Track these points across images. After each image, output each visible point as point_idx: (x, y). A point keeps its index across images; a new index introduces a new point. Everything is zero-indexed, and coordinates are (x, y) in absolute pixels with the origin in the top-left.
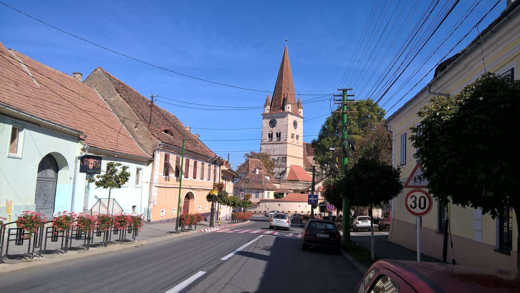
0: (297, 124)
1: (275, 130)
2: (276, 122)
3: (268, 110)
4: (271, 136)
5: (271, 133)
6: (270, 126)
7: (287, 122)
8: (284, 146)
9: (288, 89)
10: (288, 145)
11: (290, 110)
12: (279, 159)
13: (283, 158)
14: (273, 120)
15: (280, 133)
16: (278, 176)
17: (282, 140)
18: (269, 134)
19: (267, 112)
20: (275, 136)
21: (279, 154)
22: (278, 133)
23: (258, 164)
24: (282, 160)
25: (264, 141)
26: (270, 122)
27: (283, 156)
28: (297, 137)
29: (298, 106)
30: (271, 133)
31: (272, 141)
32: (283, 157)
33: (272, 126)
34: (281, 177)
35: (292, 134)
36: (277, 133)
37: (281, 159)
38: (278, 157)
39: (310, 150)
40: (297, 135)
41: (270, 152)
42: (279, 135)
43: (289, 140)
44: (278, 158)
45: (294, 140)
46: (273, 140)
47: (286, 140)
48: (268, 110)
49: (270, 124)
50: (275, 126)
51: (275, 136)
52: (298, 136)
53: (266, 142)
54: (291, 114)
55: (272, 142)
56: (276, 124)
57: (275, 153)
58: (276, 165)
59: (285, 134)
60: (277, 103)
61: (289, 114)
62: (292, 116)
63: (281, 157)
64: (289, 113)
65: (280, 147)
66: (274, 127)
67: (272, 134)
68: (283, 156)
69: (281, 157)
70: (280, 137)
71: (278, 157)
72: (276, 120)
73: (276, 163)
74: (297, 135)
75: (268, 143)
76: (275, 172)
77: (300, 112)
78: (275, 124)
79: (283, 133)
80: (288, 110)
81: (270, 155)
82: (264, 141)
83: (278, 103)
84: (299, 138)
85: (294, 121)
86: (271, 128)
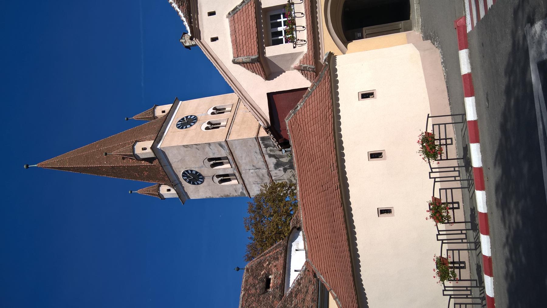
0: (187, 117)
1: (206, 171)
2: (187, 171)
3: (169, 190)
4: (225, 178)
6: (202, 182)
7: (178, 147)
8: (236, 147)
9: (106, 154)
10: (231, 138)
11: (149, 144)
12: (272, 153)
13: (266, 146)
15: (210, 160)
17: (223, 153)
18: (221, 181)
19: (173, 191)
21: (260, 156)
22: (212, 162)
23: (254, 286)
24: (272, 148)
25: (241, 190)
26: (194, 184)
27: (262, 146)
28: (219, 111)
29: (151, 119)
30: (217, 180)
31: (234, 175)
35: (207, 128)
37: (271, 150)
38: (267, 157)
40: (213, 113)
41: (263, 175)
42: (216, 162)
43: (218, 135)
44: (270, 156)
46: (230, 172)
47: (220, 145)
48: (169, 190)
49: (198, 184)
50: (197, 173)
52: (215, 109)
53: (240, 186)
54: (158, 140)
55: (237, 174)
56: (192, 171)
57: (261, 164)
58: (289, 158)
59: (207, 149)
60: (146, 174)
61: (158, 147)
62: (165, 134)
63: (264, 150)
64: (153, 148)
65: (242, 157)
66: (200, 175)
68: (262, 146)
69: (264, 150)
70: (219, 159)
71: (267, 157)
72: (184, 173)
73: (285, 160)
75: (241, 182)
77: (164, 112)
78: (194, 172)
79: (207, 153)
80: (149, 150)
81: (268, 175)
82: (241, 190)
83: (146, 171)
84: (219, 105)
85: (179, 127)
86: (205, 181)
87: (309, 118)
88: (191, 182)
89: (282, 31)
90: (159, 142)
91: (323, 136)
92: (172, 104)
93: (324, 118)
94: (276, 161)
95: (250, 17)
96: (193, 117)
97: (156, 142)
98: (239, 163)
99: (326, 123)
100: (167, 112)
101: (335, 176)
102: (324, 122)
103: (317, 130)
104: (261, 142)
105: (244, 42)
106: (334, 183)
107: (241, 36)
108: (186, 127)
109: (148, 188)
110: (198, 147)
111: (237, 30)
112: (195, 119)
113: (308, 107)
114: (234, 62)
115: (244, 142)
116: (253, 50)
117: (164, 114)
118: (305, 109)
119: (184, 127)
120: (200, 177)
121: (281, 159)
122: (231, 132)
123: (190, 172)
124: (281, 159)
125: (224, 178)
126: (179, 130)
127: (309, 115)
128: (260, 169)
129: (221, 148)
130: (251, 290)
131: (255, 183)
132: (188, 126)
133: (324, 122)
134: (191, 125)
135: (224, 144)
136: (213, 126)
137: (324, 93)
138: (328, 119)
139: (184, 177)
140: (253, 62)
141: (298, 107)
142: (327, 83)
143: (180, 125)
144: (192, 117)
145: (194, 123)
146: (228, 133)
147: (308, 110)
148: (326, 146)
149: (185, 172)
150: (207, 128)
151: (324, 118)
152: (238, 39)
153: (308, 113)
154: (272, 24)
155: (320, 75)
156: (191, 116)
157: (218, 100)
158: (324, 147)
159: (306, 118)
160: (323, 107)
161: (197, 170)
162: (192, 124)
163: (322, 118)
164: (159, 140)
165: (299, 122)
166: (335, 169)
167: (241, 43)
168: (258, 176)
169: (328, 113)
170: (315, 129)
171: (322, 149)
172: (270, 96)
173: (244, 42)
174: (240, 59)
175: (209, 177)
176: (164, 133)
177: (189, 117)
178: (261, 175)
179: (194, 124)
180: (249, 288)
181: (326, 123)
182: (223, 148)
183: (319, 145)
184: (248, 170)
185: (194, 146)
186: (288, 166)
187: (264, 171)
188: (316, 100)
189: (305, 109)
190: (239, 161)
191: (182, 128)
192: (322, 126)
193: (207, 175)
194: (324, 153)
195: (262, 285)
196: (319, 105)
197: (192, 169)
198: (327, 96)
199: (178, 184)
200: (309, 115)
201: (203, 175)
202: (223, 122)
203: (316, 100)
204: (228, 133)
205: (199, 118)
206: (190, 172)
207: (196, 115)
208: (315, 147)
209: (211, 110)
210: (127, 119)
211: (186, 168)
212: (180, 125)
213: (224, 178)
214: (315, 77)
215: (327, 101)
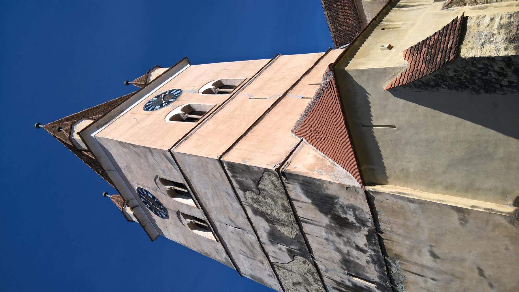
16: (361, 239)
27: (236, 185)
32: (238, 182)
34: (363, 223)
39: (348, 25)
61: (93, 135)
63: (240, 193)
69: (240, 193)
76: (338, 250)
90: (102, 126)
94: (269, 228)
97: (96, 124)
109: (115, 196)
110: (136, 149)
121: (279, 227)
124: (279, 227)
128: (244, 230)
131: (242, 253)
149: (139, 190)
164: (104, 123)
168: (243, 242)
176: (123, 111)
178: (249, 243)
184: (224, 225)
185: (131, 147)
186: (296, 248)
187: (253, 238)
199: (138, 206)
210: (127, 84)
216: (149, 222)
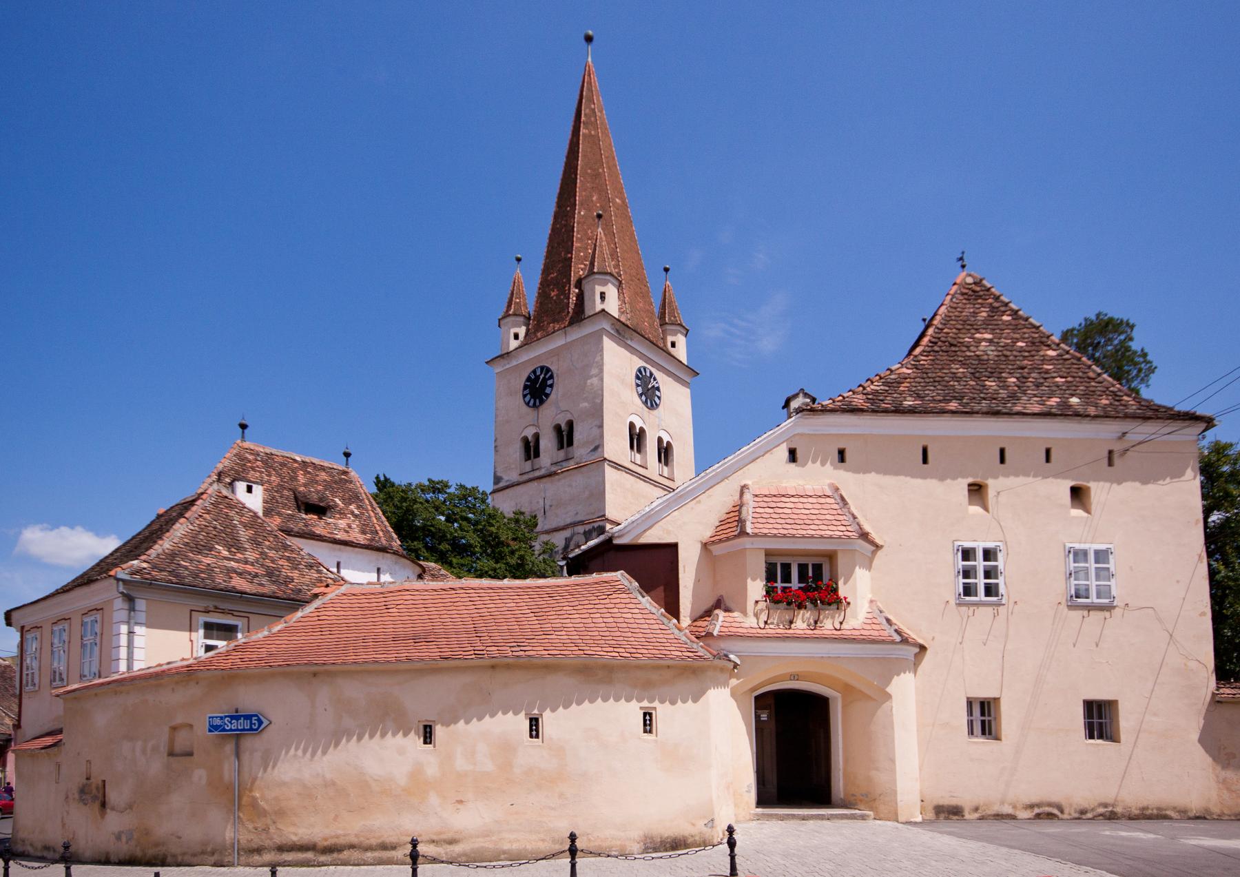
0: (658, 389)
2: (552, 377)
5: (529, 433)
6: (528, 404)
14: (538, 373)
15: (570, 424)
17: (580, 450)
18: (526, 442)
20: (548, 443)
22: (563, 426)
23: (313, 481)
26: (525, 387)
28: (665, 453)
33: (535, 403)
35: (632, 426)
36: (558, 428)
40: (660, 440)
42: (565, 436)
43: (616, 445)
45: (644, 458)
49: (525, 396)
50: (547, 396)
51: (548, 443)
56: (551, 386)
66: (542, 402)
67: (537, 437)
70: (570, 443)
74: (660, 440)
77: (673, 345)
78: (548, 390)
85: (639, 371)
87: (619, 615)
88: (529, 383)
89: (790, 582)
91: (581, 637)
92: (686, 364)
93: (615, 642)
95: (825, 527)
96: (658, 401)
98: (559, 480)
99: (605, 645)
100: (672, 350)
101: (500, 652)
102: (607, 642)
103: (595, 629)
104: (596, 525)
105: (780, 511)
106: (488, 649)
107: (792, 505)
108: (638, 385)
111: (802, 500)
112: (652, 405)
113: (640, 616)
114: (743, 489)
115: (599, 494)
116: (761, 526)
117: (669, 345)
118: (637, 611)
119: (639, 382)
120: (537, 401)
122: (619, 472)
123: (549, 382)
125: (532, 449)
126: (635, 371)
127: (624, 615)
129: (592, 447)
130: (304, 475)
132: (640, 389)
133: (607, 642)
134: (641, 395)
135: (596, 456)
136: (637, 439)
137: (663, 648)
138: (612, 649)
139: (539, 369)
140: (741, 522)
141: (643, 597)
142: (680, 654)
143: (644, 374)
144: (656, 399)
145: (645, 403)
146: (617, 466)
147: (634, 616)
148: (562, 641)
149: (550, 373)
150: (632, 426)
151: (615, 642)
152: (784, 499)
153: (629, 616)
154: (807, 565)
155: (698, 643)
156: (659, 398)
157: (684, 453)
158: (559, 637)
159: (620, 610)
160: (637, 643)
161: (552, 397)
162: (644, 398)
163: (614, 638)
165: (614, 596)
166: (514, 653)
167: (779, 505)
169: (623, 650)
170: (597, 625)
171: (556, 633)
172: (673, 547)
173: (780, 511)
174: (748, 497)
175: (536, 418)
177: (657, 393)
179: (643, 402)
180: (309, 473)
181: (605, 645)
182: (591, 451)
183: (565, 629)
188: (652, 631)
189: (637, 611)
190: (563, 481)
191: (637, 377)
192: (600, 638)
193: (540, 416)
194: (548, 637)
195: (314, 498)
196: (641, 635)
197: (555, 388)
198: (658, 652)
200: (624, 615)
201: (541, 408)
202: (641, 459)
203: (652, 631)
204: (617, 466)
205: (655, 412)
206: (549, 382)
207: (660, 407)
208: (562, 621)
209: (666, 439)
211: (557, 376)
212: (644, 374)
213: (532, 449)
214: (697, 633)
215: (646, 651)
216: (508, 363)
